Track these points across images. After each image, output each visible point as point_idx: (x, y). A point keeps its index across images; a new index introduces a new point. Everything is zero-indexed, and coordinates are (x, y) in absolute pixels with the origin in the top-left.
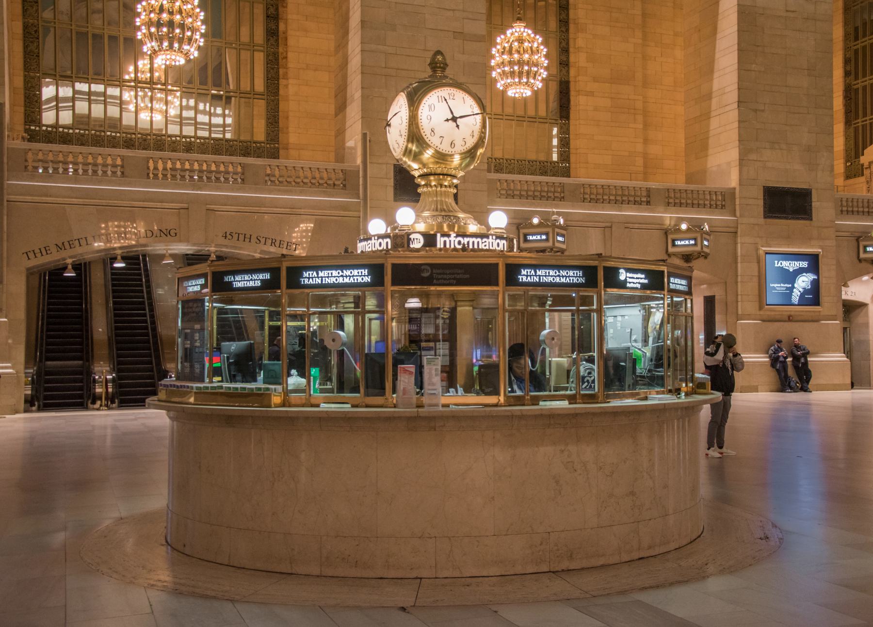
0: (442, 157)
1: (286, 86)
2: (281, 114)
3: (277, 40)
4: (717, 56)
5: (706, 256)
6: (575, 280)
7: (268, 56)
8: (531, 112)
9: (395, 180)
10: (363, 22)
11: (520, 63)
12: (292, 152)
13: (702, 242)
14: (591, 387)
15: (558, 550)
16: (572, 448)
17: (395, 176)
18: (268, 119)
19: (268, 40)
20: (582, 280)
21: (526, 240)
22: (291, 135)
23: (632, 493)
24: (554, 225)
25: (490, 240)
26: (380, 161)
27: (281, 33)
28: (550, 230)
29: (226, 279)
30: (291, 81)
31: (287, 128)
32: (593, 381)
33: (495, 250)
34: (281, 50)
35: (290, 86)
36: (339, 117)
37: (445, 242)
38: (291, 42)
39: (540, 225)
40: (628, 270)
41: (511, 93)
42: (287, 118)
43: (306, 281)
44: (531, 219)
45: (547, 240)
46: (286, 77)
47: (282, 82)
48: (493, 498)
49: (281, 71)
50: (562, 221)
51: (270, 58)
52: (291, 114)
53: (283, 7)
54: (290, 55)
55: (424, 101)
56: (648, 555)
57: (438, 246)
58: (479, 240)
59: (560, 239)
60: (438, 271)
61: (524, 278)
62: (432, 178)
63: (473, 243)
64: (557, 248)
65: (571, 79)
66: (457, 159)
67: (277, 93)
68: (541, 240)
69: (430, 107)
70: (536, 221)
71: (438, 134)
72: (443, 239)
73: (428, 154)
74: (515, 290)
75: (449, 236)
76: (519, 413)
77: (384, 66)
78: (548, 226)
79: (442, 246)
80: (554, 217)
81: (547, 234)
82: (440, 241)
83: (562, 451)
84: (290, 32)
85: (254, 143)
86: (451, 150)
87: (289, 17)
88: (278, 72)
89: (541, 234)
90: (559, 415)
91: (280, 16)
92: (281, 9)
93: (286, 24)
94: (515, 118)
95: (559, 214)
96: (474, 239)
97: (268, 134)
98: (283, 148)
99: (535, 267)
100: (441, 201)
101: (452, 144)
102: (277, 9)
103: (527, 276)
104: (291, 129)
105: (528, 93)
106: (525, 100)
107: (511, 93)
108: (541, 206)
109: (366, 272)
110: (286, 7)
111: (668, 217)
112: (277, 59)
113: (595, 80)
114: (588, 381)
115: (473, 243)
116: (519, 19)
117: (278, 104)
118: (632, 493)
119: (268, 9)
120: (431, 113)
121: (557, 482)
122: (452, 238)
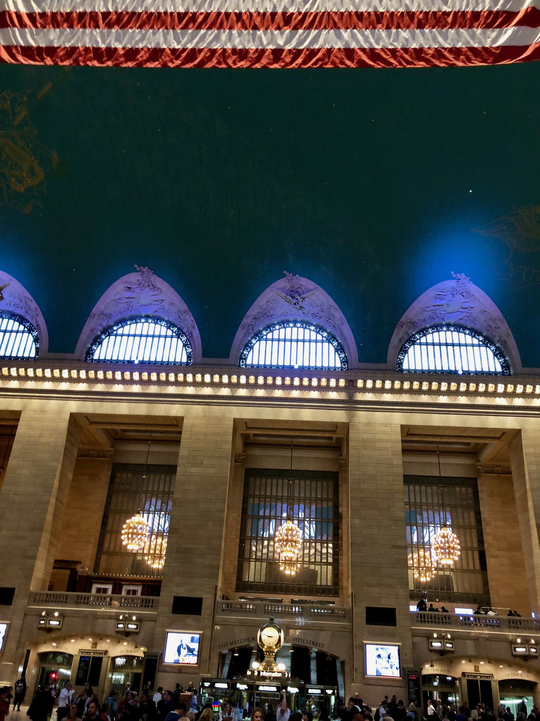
4: (533, 548)
5: (536, 657)
8: (465, 567)
13: (529, 650)
65: (486, 549)
111: (510, 634)
113: (499, 549)
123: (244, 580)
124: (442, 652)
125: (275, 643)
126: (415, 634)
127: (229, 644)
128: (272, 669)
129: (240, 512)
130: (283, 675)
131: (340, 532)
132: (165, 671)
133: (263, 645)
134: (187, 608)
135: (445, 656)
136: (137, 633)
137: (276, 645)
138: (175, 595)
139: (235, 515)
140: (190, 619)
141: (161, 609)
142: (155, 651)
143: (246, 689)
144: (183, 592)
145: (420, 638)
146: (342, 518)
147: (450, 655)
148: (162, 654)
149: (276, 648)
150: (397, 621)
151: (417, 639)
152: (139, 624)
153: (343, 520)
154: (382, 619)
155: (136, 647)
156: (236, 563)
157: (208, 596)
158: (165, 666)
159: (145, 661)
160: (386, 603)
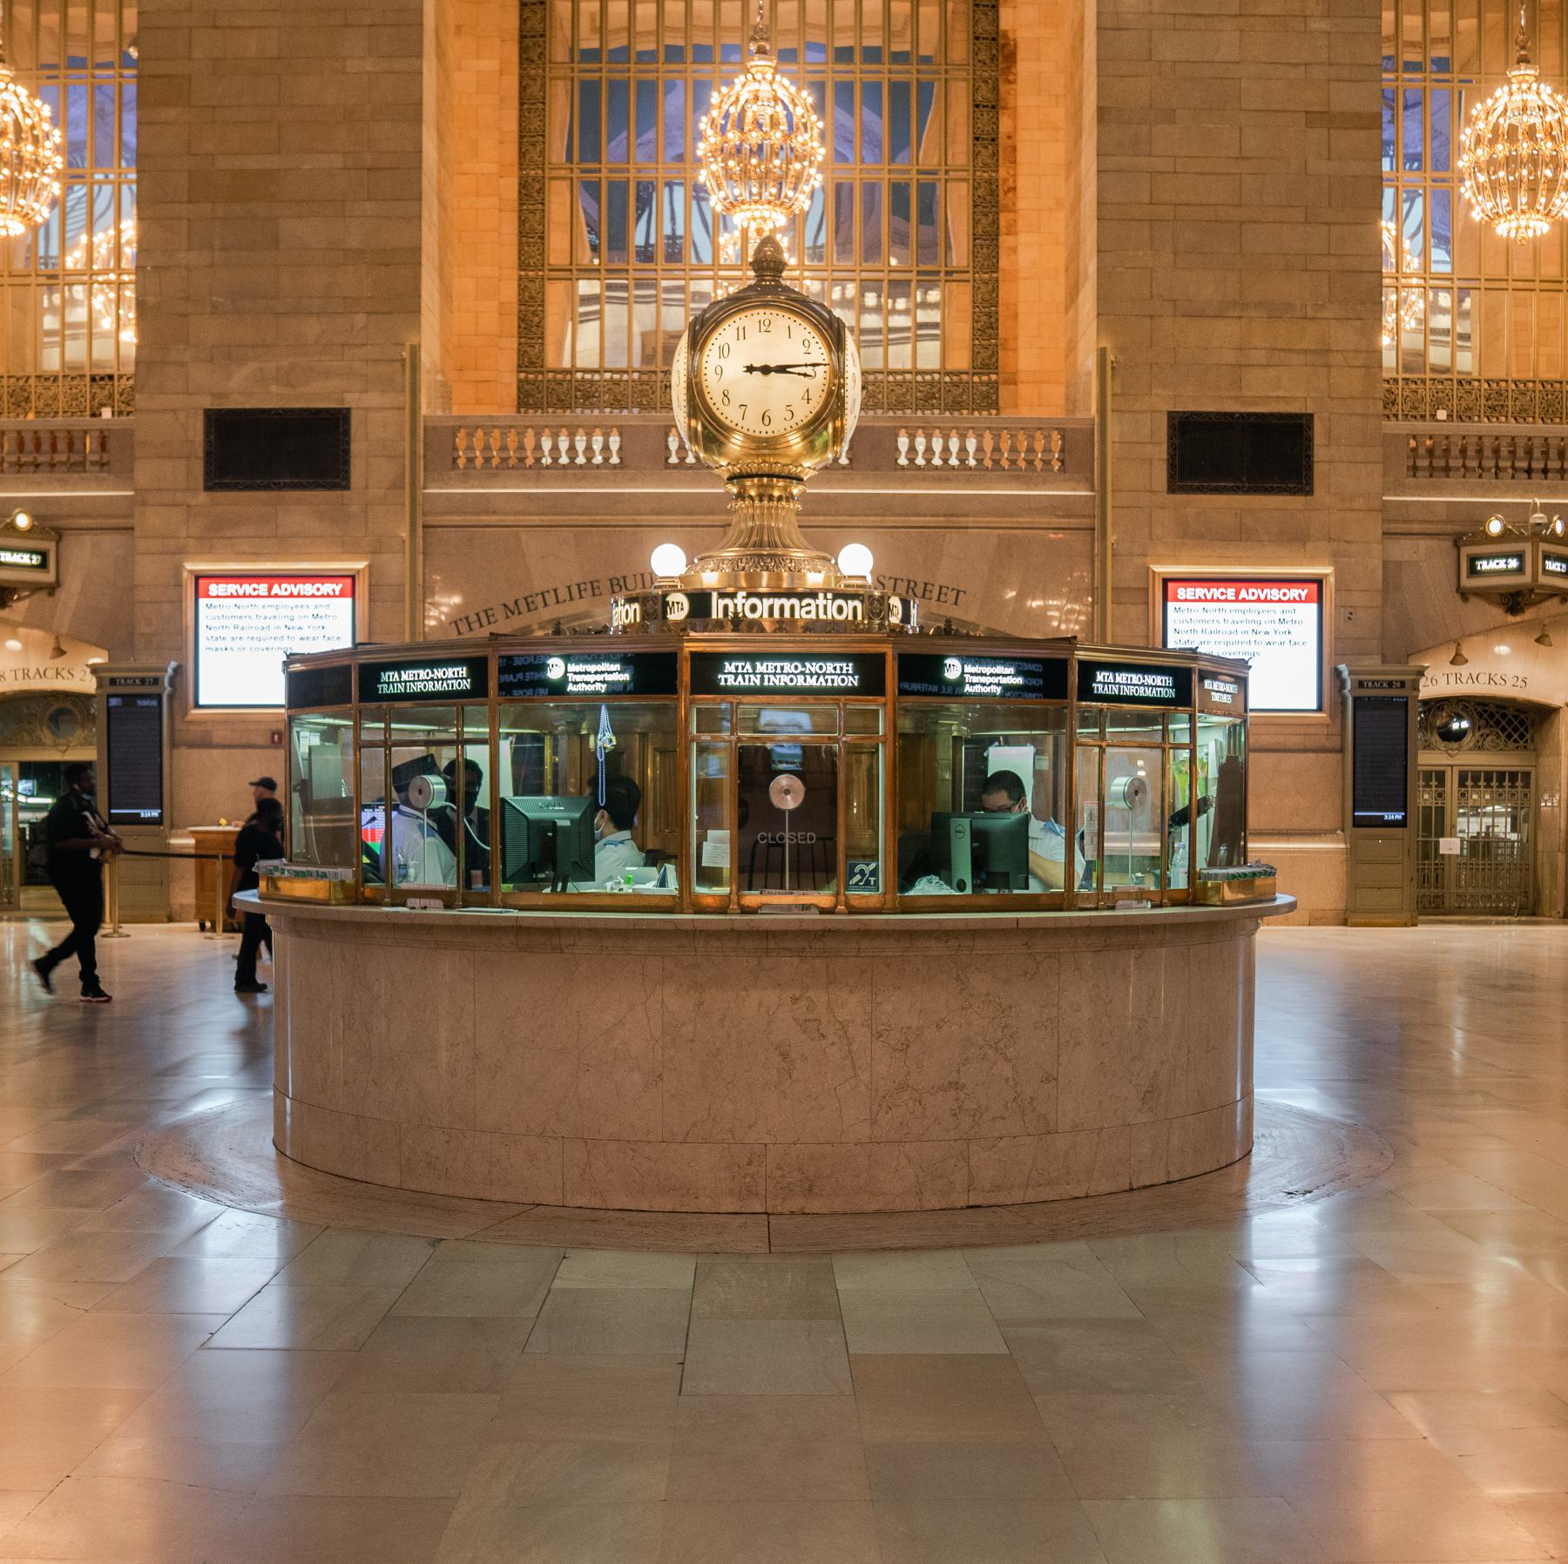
0: (765, 445)
1: (1014, 250)
2: (1001, 309)
3: (995, 154)
6: (838, 682)
7: (975, 188)
9: (1171, 445)
10: (1102, 112)
11: (1534, 161)
12: (1024, 389)
14: (868, 883)
15: (783, 1176)
16: (819, 996)
17: (1170, 437)
18: (975, 321)
19: (976, 155)
20: (853, 681)
21: (1473, 571)
22: (1021, 352)
23: (956, 1086)
24: (1539, 534)
25: (821, 601)
26: (1137, 406)
27: (1002, 140)
28: (1527, 547)
29: (626, 677)
30: (1023, 238)
31: (1016, 338)
32: (874, 873)
33: (834, 621)
34: (1002, 173)
35: (1020, 250)
36: (1071, 313)
37: (726, 607)
38: (1023, 155)
39: (1506, 536)
40: (966, 659)
41: (1502, 229)
42: (1015, 316)
43: (731, 681)
44: (1484, 522)
45: (1520, 570)
46: (1012, 230)
47: (1005, 241)
48: (660, 1076)
49: (1004, 219)
50: (1559, 527)
51: (980, 192)
52: (1022, 308)
53: (1010, 82)
54: (1022, 183)
55: (712, 340)
56: (993, 1202)
57: (714, 616)
58: (795, 601)
59: (1553, 566)
60: (581, 668)
61: (731, 679)
62: (748, 483)
63: (782, 608)
64: (1542, 586)
66: (796, 442)
67: (995, 268)
68: (1506, 572)
69: (721, 349)
70: (1495, 527)
71: (735, 402)
72: (722, 602)
73: (736, 443)
74: (706, 701)
75: (733, 596)
76: (689, 927)
77: (1146, 200)
78: (1521, 538)
79: (721, 616)
80: (1538, 517)
81: (1520, 556)
82: (717, 608)
83: (795, 1000)
84: (1022, 135)
85: (947, 374)
86: (764, 429)
87: (1021, 101)
88: (996, 222)
89: (1507, 556)
90: (785, 932)
91: (1002, 104)
92: (1003, 88)
93: (1014, 118)
94: (1537, 285)
95: (1548, 509)
96: (783, 601)
97: (975, 354)
98: (1006, 383)
99: (753, 657)
100: (770, 527)
101: (765, 418)
102: (996, 89)
103: (736, 675)
104: (1022, 342)
105: (1542, 227)
106: (1536, 245)
107: (1502, 229)
108: (1514, 493)
109: (463, 671)
110: (1014, 82)
112: (994, 193)
114: (862, 872)
115: (782, 608)
116: (1524, 60)
117: (996, 289)
118: (956, 1086)
119: (976, 90)
120: (722, 362)
121: (784, 1056)
122: (739, 600)
123: (550, 362)
124: (1514, 600)
125: (805, 413)
126: (1396, 526)
127: (500, 614)
128: (796, 572)
129: (513, 51)
130: (871, 614)
131: (1005, 125)
132: (205, 743)
133: (713, 434)
134: (277, 454)
135: (1529, 614)
136: (52, 589)
137: (812, 427)
138: (208, 403)
139: (491, 65)
140: (298, 508)
141: (145, 472)
142: (144, 661)
143: (615, 691)
144: (248, 389)
145: (1423, 544)
146: (1012, 58)
147: (1553, 606)
148: (179, 670)
149: (811, 449)
150: (1318, 469)
151: (1404, 550)
152: (50, 546)
153: (1024, 67)
154: (1241, 456)
155: (59, 652)
156: (510, 292)
157: (374, 399)
158: (201, 722)
159: (97, 708)
160: (1268, 392)
